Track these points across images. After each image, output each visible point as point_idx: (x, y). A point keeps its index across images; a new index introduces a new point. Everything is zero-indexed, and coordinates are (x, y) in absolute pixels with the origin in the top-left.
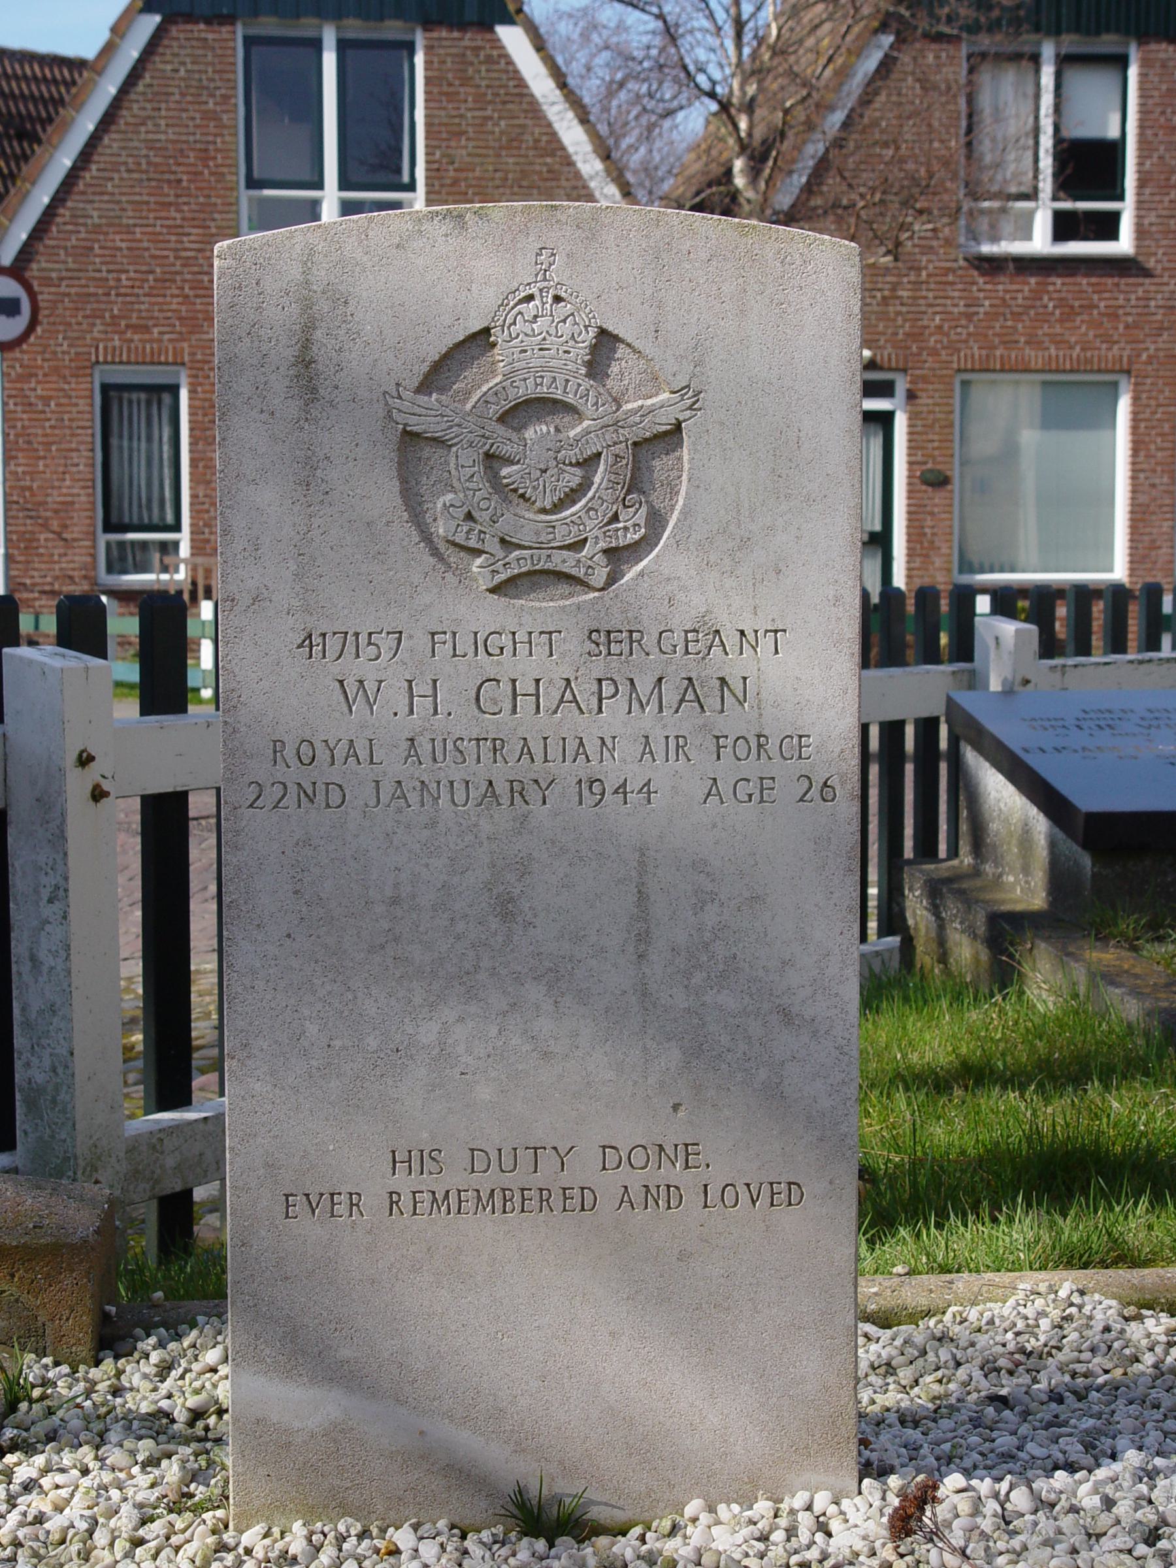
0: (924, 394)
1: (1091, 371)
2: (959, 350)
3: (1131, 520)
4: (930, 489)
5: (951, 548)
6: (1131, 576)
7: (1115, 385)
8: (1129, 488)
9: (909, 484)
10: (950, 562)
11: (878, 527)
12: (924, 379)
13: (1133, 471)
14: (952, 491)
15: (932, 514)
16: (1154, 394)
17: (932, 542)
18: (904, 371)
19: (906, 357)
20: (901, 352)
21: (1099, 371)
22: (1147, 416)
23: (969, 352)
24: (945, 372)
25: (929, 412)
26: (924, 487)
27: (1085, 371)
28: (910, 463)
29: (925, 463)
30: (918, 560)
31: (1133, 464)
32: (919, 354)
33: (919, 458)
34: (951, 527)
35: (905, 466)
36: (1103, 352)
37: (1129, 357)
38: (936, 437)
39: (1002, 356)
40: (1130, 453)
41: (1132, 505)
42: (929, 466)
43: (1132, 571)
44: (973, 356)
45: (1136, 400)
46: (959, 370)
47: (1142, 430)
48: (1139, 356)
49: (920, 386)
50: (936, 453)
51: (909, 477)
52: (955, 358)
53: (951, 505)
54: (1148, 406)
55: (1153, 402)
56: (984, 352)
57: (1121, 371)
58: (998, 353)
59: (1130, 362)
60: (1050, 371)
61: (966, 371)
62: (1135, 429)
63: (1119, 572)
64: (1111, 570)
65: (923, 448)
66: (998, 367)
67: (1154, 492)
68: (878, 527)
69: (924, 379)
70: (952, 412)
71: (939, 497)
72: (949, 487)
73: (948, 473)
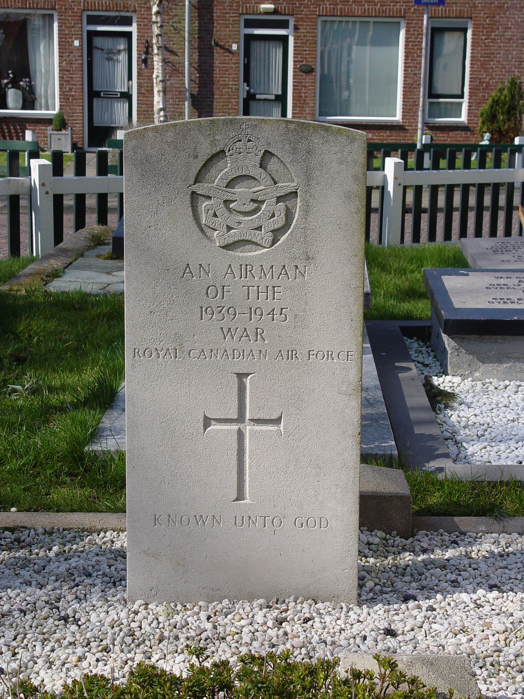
0: (302, 27)
1: (386, 17)
2: (319, 5)
3: (404, 91)
4: (304, 74)
5: (314, 103)
6: (403, 119)
7: (399, 23)
8: (403, 75)
9: (294, 72)
10: (314, 110)
11: (280, 93)
12: (302, 19)
13: (405, 67)
14: (315, 76)
15: (305, 87)
16: (416, 29)
17: (305, 100)
18: (293, 15)
19: (293, 8)
20: (290, 6)
21: (389, 17)
22: (413, 39)
23: (324, 6)
24: (312, 16)
25: (305, 36)
26: (301, 73)
27: (382, 17)
28: (294, 61)
29: (302, 61)
30: (298, 109)
31: (405, 63)
32: (300, 7)
33: (299, 59)
34: (315, 93)
35: (292, 63)
36: (392, 7)
37: (405, 10)
38: (307, 49)
39: (341, 8)
40: (404, 58)
41: (404, 84)
42: (304, 63)
43: (404, 116)
44: (326, 8)
45: (407, 32)
46: (319, 15)
47: (410, 47)
48: (410, 9)
49: (300, 23)
50: (308, 56)
51: (294, 68)
52: (318, 9)
53: (315, 83)
54: (414, 34)
55: (416, 33)
56: (332, 7)
57: (400, 17)
58: (339, 7)
59: (405, 12)
60: (365, 16)
61: (323, 15)
62: (406, 46)
63: (398, 117)
64: (395, 116)
65: (300, 54)
66: (339, 14)
67: (415, 78)
68: (280, 93)
69: (302, 19)
70: (316, 36)
71: (308, 79)
72: (314, 74)
73: (313, 67)
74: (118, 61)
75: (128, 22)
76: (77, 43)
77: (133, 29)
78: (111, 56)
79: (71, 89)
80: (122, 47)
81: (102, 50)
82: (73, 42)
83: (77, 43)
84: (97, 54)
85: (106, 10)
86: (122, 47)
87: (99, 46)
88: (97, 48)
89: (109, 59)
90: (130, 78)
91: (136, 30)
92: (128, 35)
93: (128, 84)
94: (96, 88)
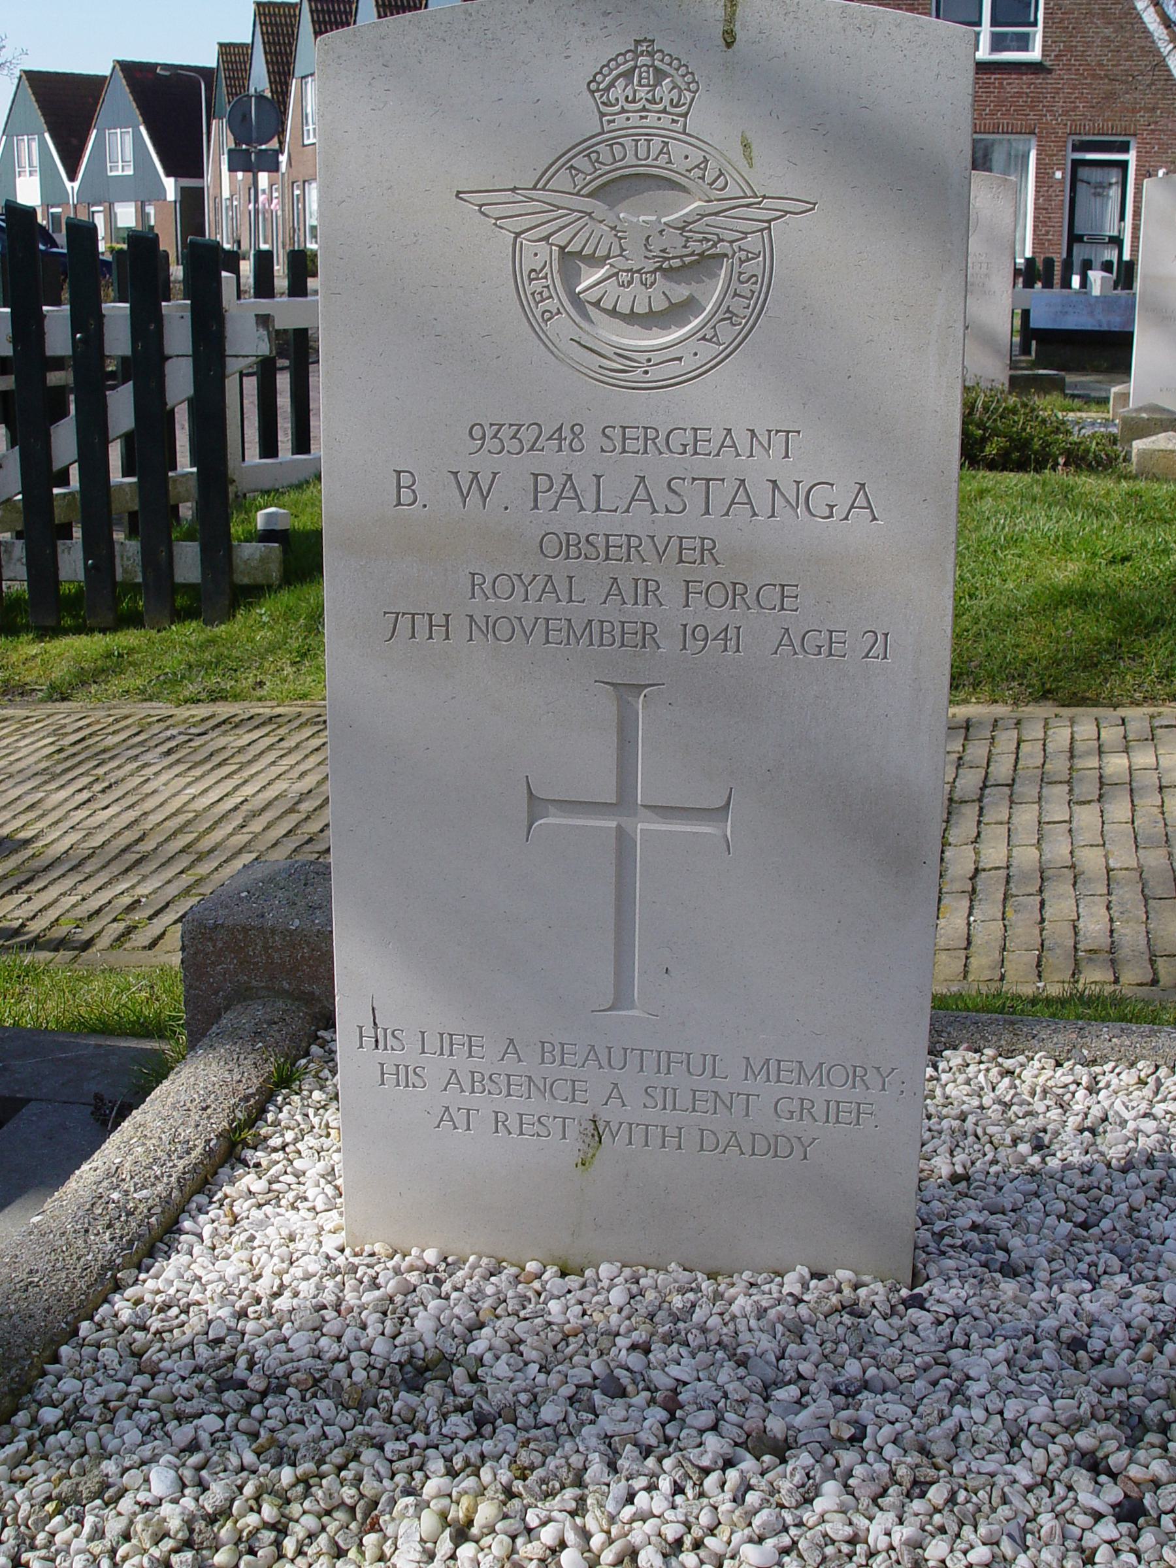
74: (1108, 196)
75: (1124, 148)
76: (1058, 175)
77: (1131, 157)
78: (1100, 189)
79: (1047, 233)
80: (1114, 180)
81: (1089, 183)
82: (1054, 173)
83: (1058, 175)
84: (1082, 188)
85: (1098, 134)
86: (1114, 180)
87: (1085, 178)
88: (1082, 181)
89: (1096, 195)
90: (1122, 218)
91: (1134, 158)
92: (1124, 165)
93: (1120, 226)
94: (1078, 231)
